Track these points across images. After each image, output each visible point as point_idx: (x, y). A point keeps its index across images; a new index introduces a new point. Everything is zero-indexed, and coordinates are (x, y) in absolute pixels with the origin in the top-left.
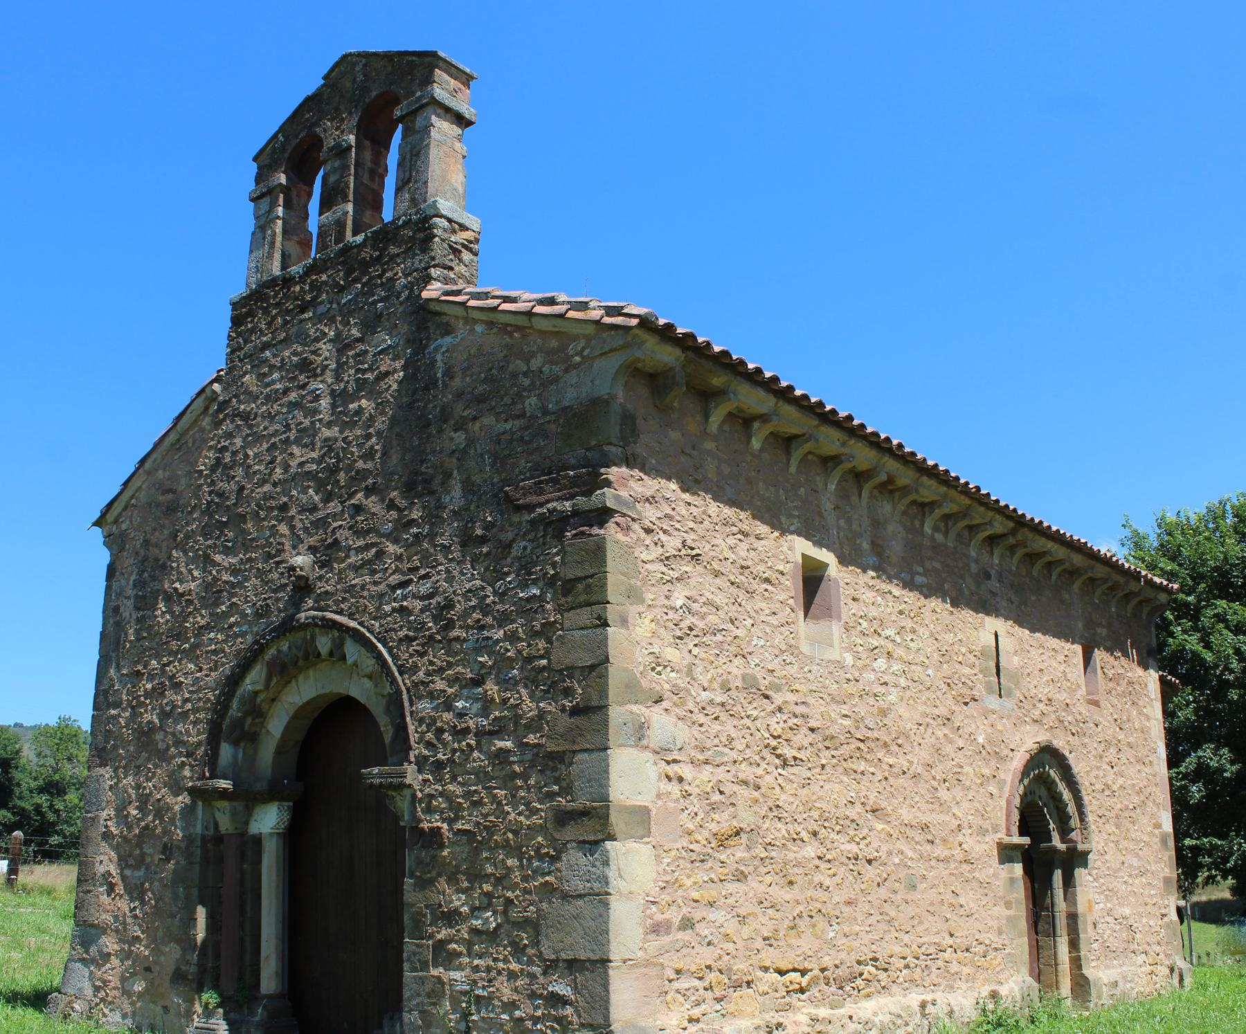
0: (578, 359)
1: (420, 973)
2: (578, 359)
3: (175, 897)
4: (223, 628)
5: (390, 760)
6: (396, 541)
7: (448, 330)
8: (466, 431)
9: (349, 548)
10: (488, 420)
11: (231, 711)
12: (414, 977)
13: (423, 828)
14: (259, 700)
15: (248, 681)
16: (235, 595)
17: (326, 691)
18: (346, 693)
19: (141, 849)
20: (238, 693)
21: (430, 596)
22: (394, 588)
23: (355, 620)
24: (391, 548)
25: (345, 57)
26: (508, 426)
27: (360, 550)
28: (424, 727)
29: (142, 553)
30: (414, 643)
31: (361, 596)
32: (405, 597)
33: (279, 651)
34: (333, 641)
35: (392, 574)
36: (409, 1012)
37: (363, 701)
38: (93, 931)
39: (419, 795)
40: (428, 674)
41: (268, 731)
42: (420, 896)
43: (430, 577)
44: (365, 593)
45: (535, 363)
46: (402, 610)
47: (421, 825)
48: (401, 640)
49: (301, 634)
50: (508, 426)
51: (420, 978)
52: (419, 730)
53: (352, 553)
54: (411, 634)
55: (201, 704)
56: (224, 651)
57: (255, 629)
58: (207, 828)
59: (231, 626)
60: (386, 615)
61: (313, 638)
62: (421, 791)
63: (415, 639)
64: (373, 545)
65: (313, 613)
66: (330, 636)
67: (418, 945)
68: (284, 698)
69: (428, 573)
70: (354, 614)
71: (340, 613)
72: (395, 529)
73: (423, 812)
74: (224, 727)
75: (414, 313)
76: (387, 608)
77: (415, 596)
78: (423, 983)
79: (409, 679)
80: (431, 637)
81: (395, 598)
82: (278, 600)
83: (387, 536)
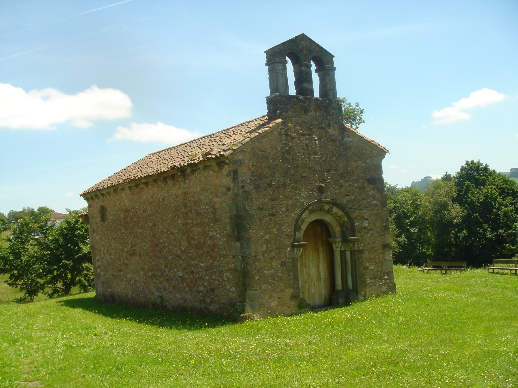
0: (376, 155)
2: (376, 155)
3: (290, 276)
7: (349, 137)
8: (356, 163)
10: (360, 162)
15: (303, 215)
17: (319, 218)
19: (271, 264)
25: (303, 35)
26: (364, 165)
29: (253, 169)
34: (330, 207)
37: (329, 221)
38: (256, 292)
45: (368, 152)
50: (364, 165)
57: (307, 201)
61: (324, 205)
75: (340, 128)
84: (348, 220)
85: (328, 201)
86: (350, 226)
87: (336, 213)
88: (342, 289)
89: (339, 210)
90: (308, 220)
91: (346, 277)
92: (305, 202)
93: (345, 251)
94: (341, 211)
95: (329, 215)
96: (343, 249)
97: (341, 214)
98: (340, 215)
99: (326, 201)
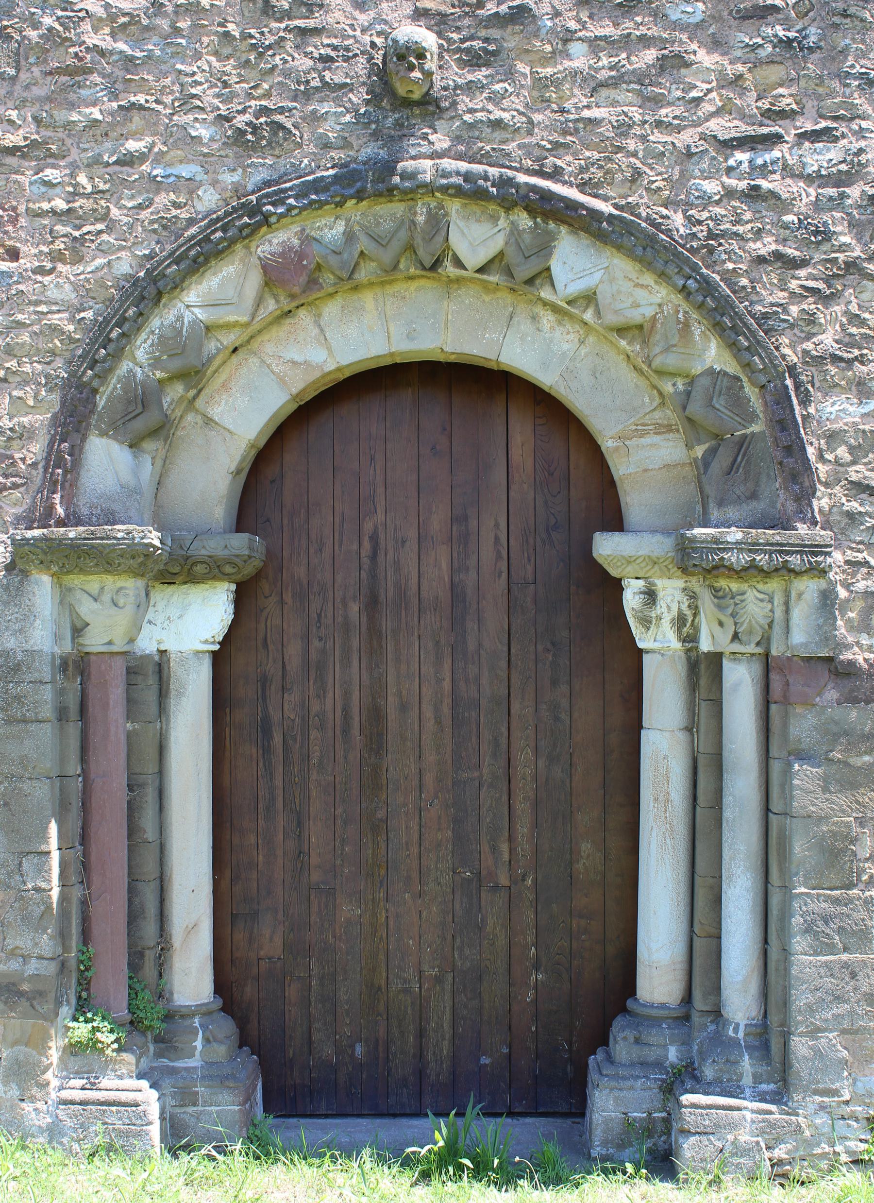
1: (845, 957)
4: (96, 161)
5: (715, 514)
6: (716, 44)
9: (568, 37)
11: (125, 366)
12: (826, 964)
13: (851, 663)
14: (211, 346)
16: (142, 86)
18: (493, 357)
20: (155, 323)
21: (841, 180)
22: (729, 145)
23: (606, 199)
24: (705, 58)
27: (596, 44)
28: (842, 452)
30: (802, 273)
31: (619, 149)
32: (764, 170)
33: (307, 239)
35: (713, 115)
36: (814, 1032)
39: (843, 593)
40: (850, 342)
41: (209, 421)
42: (842, 800)
43: (836, 139)
44: (631, 144)
46: (754, 194)
47: (846, 656)
48: (761, 260)
49: (398, 208)
51: (845, 965)
52: (829, 456)
53: (577, 48)
54: (791, 252)
55: (25, 338)
56: (105, 216)
57: (229, 178)
58: (57, 638)
59: (129, 161)
60: (707, 201)
62: (847, 586)
63: (804, 263)
64: (646, 41)
65: (448, 164)
66: (502, 223)
67: (836, 901)
68: (269, 348)
69: (827, 130)
70: (599, 185)
71: (556, 174)
72: (716, 18)
73: (851, 627)
74: (101, 401)
76: (711, 187)
77: (788, 171)
78: (853, 975)
79: (792, 346)
80: (852, 266)
81: (729, 170)
82: (315, 118)
83: (695, 30)
84: (732, 367)
85: (468, 177)
86: (756, 428)
87: (589, 298)
88: (688, 998)
89: (622, 265)
90: (294, 354)
91: (717, 901)
92: (214, 183)
93: (716, 659)
94: (648, 279)
95: (547, 318)
96: (705, 645)
97: (649, 312)
98: (636, 316)
99: (445, 174)
